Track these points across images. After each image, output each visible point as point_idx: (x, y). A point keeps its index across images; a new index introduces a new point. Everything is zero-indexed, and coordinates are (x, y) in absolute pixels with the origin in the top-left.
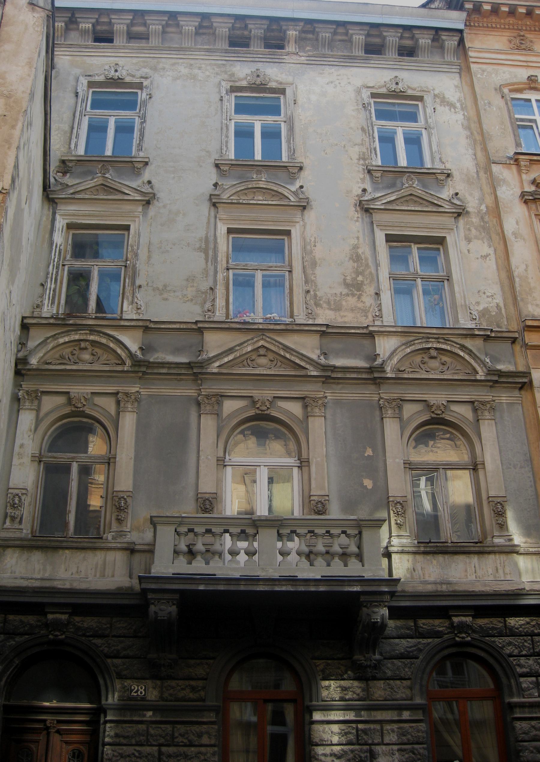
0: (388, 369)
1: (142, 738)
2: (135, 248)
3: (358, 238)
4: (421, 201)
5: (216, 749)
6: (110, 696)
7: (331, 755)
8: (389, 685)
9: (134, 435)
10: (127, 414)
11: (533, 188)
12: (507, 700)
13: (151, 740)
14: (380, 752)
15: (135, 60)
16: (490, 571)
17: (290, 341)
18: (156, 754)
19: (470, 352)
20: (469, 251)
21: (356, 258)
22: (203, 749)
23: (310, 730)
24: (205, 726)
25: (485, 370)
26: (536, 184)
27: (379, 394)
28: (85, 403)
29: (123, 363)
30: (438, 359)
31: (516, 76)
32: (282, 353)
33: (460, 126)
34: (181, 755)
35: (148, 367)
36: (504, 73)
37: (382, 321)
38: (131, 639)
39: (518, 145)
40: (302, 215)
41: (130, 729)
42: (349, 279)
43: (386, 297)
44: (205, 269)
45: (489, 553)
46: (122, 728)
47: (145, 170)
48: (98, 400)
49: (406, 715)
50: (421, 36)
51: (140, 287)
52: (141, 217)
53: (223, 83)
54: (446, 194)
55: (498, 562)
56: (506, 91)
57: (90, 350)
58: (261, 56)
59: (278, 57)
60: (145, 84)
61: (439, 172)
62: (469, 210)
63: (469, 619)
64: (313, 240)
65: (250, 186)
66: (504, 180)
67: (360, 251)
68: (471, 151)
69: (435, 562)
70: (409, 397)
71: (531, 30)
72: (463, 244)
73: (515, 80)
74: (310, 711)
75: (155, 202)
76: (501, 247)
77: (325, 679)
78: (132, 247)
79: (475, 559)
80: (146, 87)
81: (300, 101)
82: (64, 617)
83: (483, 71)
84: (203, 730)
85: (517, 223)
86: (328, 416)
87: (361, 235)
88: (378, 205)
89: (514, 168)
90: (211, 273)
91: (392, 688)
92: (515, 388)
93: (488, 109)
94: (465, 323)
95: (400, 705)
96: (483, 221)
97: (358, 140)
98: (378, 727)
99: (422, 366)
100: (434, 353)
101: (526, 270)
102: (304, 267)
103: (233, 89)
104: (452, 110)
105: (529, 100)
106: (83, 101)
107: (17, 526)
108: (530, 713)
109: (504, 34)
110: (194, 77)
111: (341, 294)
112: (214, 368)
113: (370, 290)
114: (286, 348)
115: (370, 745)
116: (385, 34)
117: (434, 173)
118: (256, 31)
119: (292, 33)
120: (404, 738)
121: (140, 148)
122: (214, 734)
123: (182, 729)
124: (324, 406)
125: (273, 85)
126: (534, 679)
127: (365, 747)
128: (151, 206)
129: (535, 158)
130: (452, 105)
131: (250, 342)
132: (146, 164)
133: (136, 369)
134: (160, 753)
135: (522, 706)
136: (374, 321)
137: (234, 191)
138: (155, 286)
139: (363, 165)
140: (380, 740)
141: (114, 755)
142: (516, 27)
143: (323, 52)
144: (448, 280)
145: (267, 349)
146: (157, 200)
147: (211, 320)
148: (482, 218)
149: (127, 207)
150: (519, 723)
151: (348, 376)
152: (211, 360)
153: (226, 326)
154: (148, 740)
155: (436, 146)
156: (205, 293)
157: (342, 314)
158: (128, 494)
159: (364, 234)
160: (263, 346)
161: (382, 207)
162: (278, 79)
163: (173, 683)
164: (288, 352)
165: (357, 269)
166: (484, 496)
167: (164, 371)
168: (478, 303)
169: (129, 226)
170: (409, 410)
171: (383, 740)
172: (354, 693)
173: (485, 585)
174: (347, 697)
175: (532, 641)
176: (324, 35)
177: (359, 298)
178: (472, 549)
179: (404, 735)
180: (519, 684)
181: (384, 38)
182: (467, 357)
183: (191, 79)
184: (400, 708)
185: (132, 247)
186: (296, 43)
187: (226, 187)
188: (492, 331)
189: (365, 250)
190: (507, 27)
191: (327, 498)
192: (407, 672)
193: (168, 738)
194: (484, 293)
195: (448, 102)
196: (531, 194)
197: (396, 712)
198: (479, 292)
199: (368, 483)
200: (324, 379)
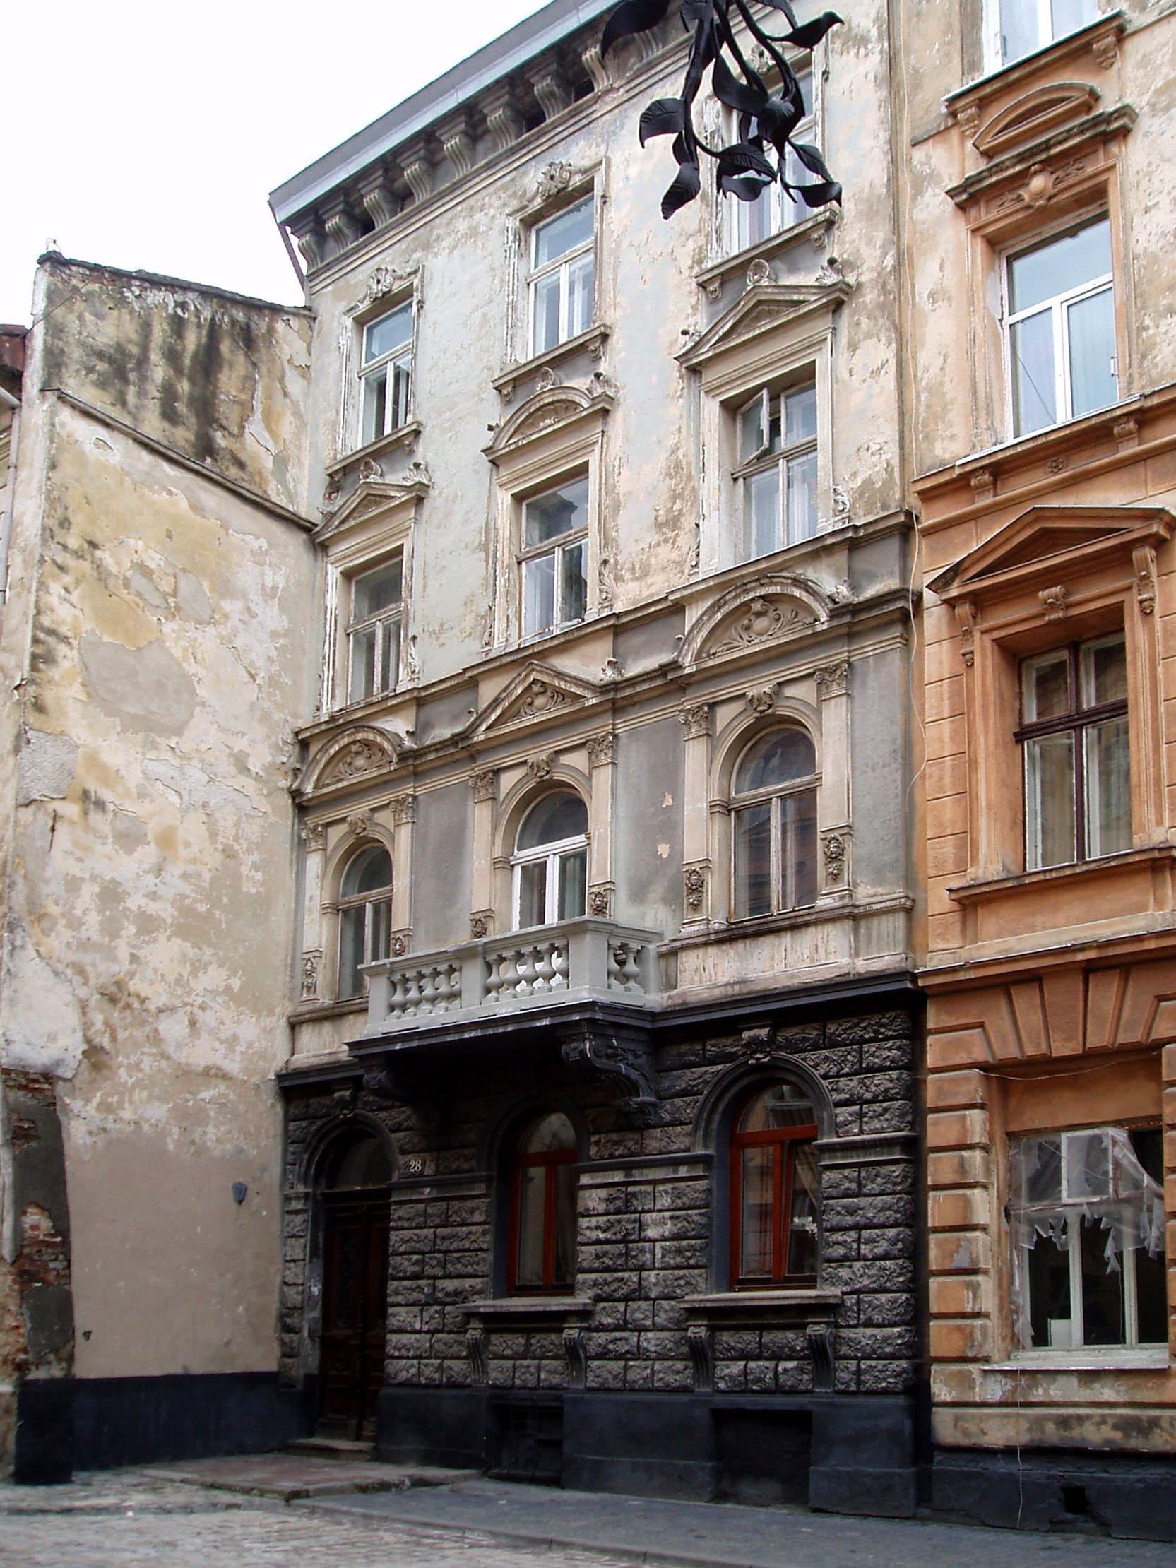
21: (675, 470)
40: (605, 424)
81: (613, 194)
87: (684, 423)
108: (843, 1157)
113: (688, 522)
123: (456, 1205)
125: (577, 180)
134: (436, 1236)
177: (673, 543)
189: (687, 450)
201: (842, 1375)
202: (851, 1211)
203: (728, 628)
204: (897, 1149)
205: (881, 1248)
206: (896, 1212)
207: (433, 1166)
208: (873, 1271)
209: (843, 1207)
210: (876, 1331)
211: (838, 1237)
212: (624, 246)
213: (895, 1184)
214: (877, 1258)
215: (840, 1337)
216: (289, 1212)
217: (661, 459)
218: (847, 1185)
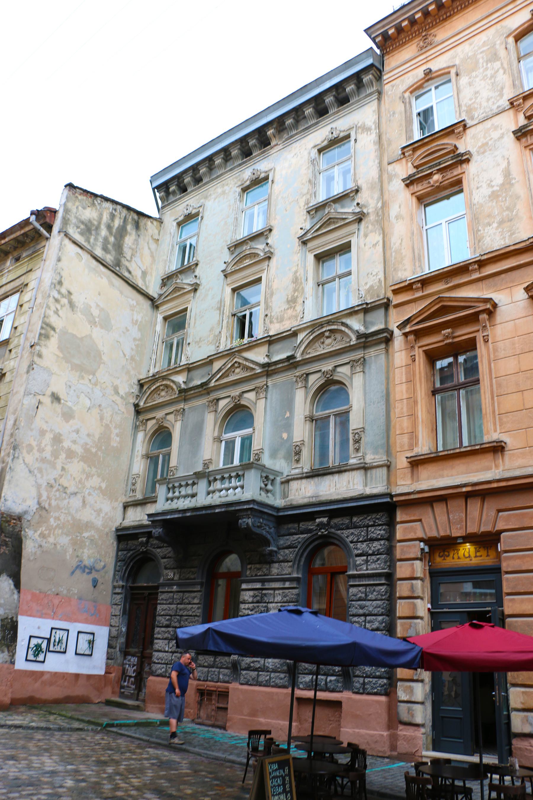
4: (336, 220)
7: (248, 609)
15: (197, 197)
16: (345, 484)
18: (175, 609)
21: (296, 280)
22: (194, 606)
35: (185, 392)
40: (269, 262)
42: (290, 296)
45: (345, 471)
49: (287, 585)
51: (189, 344)
56: (407, 95)
60: (201, 210)
63: (325, 520)
68: (377, 161)
69: (312, 482)
70: (312, 370)
77: (249, 564)
79: (336, 477)
82: (144, 539)
85: (400, 207)
86: (269, 396)
88: (309, 236)
97: (305, 191)
98: (272, 592)
99: (322, 346)
101: (401, 244)
106: (173, 237)
107: (134, 494)
108: (359, 581)
110: (224, 193)
112: (212, 384)
113: (300, 301)
114: (246, 359)
123: (187, 595)
124: (266, 390)
125: (263, 175)
126: (365, 558)
127: (264, 605)
129: (416, 145)
130: (369, 129)
135: (354, 577)
145: (239, 363)
148: (377, 213)
152: (210, 380)
157: (284, 323)
160: (236, 362)
167: (192, 392)
168: (366, 284)
170: (312, 379)
173: (338, 494)
175: (367, 531)
184: (284, 580)
186: (275, 137)
188: (367, 304)
189: (301, 272)
199: (285, 436)
202: (362, 607)
203: (315, 342)
204: (383, 578)
205: (376, 625)
206: (383, 608)
207: (178, 576)
209: (359, 605)
216: (115, 593)
217: (290, 276)
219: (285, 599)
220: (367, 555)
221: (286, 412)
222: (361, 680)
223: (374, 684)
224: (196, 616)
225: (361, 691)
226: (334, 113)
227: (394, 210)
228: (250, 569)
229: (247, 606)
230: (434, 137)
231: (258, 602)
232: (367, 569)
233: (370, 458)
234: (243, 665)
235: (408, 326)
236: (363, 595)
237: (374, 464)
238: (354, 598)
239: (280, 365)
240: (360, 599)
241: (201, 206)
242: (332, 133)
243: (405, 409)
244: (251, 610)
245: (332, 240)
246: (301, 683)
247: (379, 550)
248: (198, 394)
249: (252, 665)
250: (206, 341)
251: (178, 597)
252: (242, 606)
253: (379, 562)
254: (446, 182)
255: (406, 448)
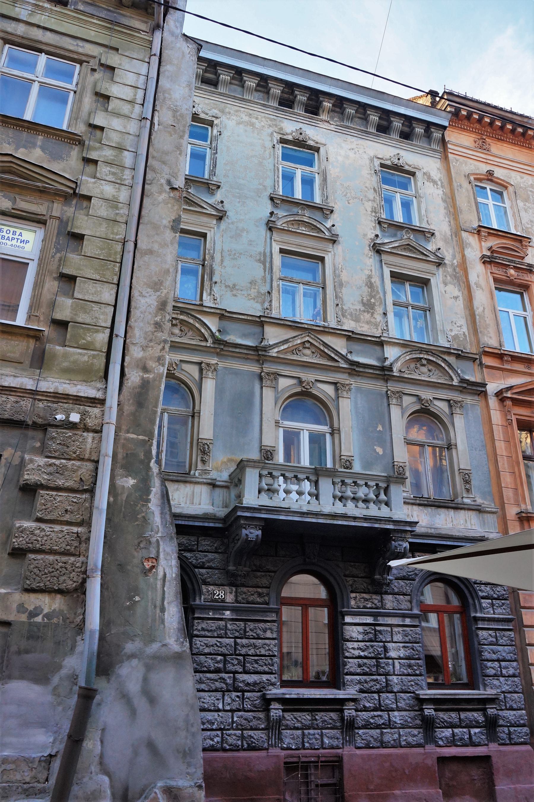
0: (395, 369)
1: (222, 632)
2: (212, 252)
3: (371, 271)
4: (415, 251)
5: (276, 641)
6: (197, 598)
7: (358, 649)
8: (396, 598)
9: (214, 396)
10: (209, 379)
11: (488, 253)
12: (473, 615)
13: (229, 634)
14: (391, 648)
15: (207, 101)
16: (462, 522)
17: (328, 339)
18: (233, 644)
19: (449, 365)
20: (445, 291)
21: (370, 285)
22: (267, 641)
23: (342, 629)
24: (269, 624)
25: (458, 378)
26: (491, 250)
27: (387, 387)
28: (175, 368)
29: (207, 341)
30: (427, 366)
31: (478, 169)
32: (322, 348)
33: (441, 199)
34: (251, 645)
36: (471, 165)
37: (388, 334)
38: (213, 554)
39: (479, 220)
40: (333, 247)
41: (213, 625)
43: (391, 316)
44: (263, 277)
45: (461, 509)
46: (207, 623)
47: (217, 191)
48: (185, 366)
49: (408, 621)
50: (417, 126)
51: (216, 283)
52: (216, 228)
53: (275, 134)
54: (431, 247)
55: (467, 516)
56: (472, 178)
57: (179, 327)
58: (302, 118)
59: (315, 121)
60: (216, 122)
61: (427, 230)
62: (446, 261)
64: (340, 267)
65: (297, 219)
66: (470, 244)
67: (373, 280)
69: (426, 511)
71: (489, 136)
72: (441, 286)
73: (478, 172)
74: (343, 615)
75: (225, 218)
76: (466, 292)
77: (352, 592)
78: (209, 250)
79: (452, 512)
80: (216, 125)
83: (457, 160)
84: (268, 627)
85: (478, 277)
88: (386, 248)
89: (476, 236)
90: (268, 280)
91: (398, 601)
92: (476, 394)
93: (460, 189)
94: (443, 342)
95: (404, 614)
96: (455, 272)
97: (371, 197)
98: (389, 629)
100: (424, 362)
101: (484, 311)
102: (335, 286)
103: (283, 141)
104: (435, 186)
105: (486, 188)
108: (488, 625)
109: (471, 135)
110: (252, 125)
111: (360, 310)
113: (380, 310)
114: (326, 345)
115: (384, 642)
116: (392, 119)
117: (424, 231)
118: (301, 97)
119: (327, 104)
120: (406, 638)
121: (213, 172)
122: (275, 630)
123: (252, 625)
126: (490, 601)
127: (381, 644)
128: (222, 221)
129: (492, 231)
131: (300, 337)
132: (219, 187)
133: (216, 346)
134: (236, 644)
135: (483, 619)
136: (382, 333)
137: (285, 220)
138: (227, 284)
139: (375, 217)
140: (391, 639)
141: (201, 645)
142: (480, 132)
143: (347, 124)
144: (429, 311)
145: (311, 344)
146: (227, 218)
147: (269, 316)
148: (454, 270)
149: (205, 219)
150: (481, 631)
151: (367, 370)
153: (282, 322)
154: (226, 633)
155: (424, 211)
156: (265, 294)
158: (210, 441)
159: (375, 269)
160: (308, 341)
161: (389, 250)
162: (314, 139)
163: (245, 589)
164: (326, 348)
165: (371, 294)
166: (456, 468)
168: (451, 330)
169: (206, 234)
170: (406, 400)
171: (392, 640)
172: (373, 603)
173: (459, 531)
174: (368, 606)
176: (350, 110)
177: (372, 314)
178: (450, 505)
179: (407, 636)
180: (480, 604)
181: (391, 122)
182: (447, 368)
183: (250, 126)
184: (404, 616)
185: (209, 250)
186: (328, 113)
187: (280, 216)
188: (462, 351)
189: (376, 280)
190: (474, 130)
191: (353, 458)
192: (408, 590)
193: (242, 632)
194: (455, 324)
195: (432, 180)
196: (489, 257)
197: (401, 619)
198: (452, 322)
199: (379, 450)
200: (350, 371)
201: (501, 735)
205: (511, 671)
206: (515, 654)
208: (509, 683)
209: (492, 650)
210: (515, 712)
211: (489, 664)
212: (338, 184)
213: (512, 641)
214: (509, 676)
215: (499, 715)
217: (364, 277)
218: (491, 639)
219: (407, 639)
220: (493, 599)
221: (377, 424)
222: (506, 730)
223: (519, 733)
224: (274, 656)
225: (508, 742)
226: (397, 140)
227: (473, 278)
228: (355, 598)
229: (356, 645)
230: (506, 235)
231: (370, 641)
232: (494, 613)
233: (479, 501)
234: (360, 722)
235: (509, 392)
236: (494, 640)
237: (487, 509)
238: (485, 642)
239: (371, 371)
240: (491, 644)
241: (217, 118)
242: (399, 159)
243: (506, 466)
244: (363, 651)
245: (412, 267)
246: (441, 738)
247: (503, 595)
248: (244, 356)
249: (372, 721)
250: (244, 292)
251: (235, 627)
252: (350, 645)
253: (504, 607)
254: (519, 281)
255: (512, 502)
